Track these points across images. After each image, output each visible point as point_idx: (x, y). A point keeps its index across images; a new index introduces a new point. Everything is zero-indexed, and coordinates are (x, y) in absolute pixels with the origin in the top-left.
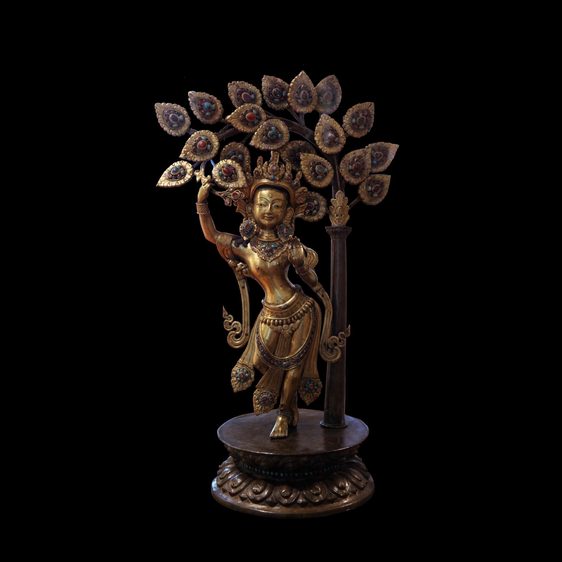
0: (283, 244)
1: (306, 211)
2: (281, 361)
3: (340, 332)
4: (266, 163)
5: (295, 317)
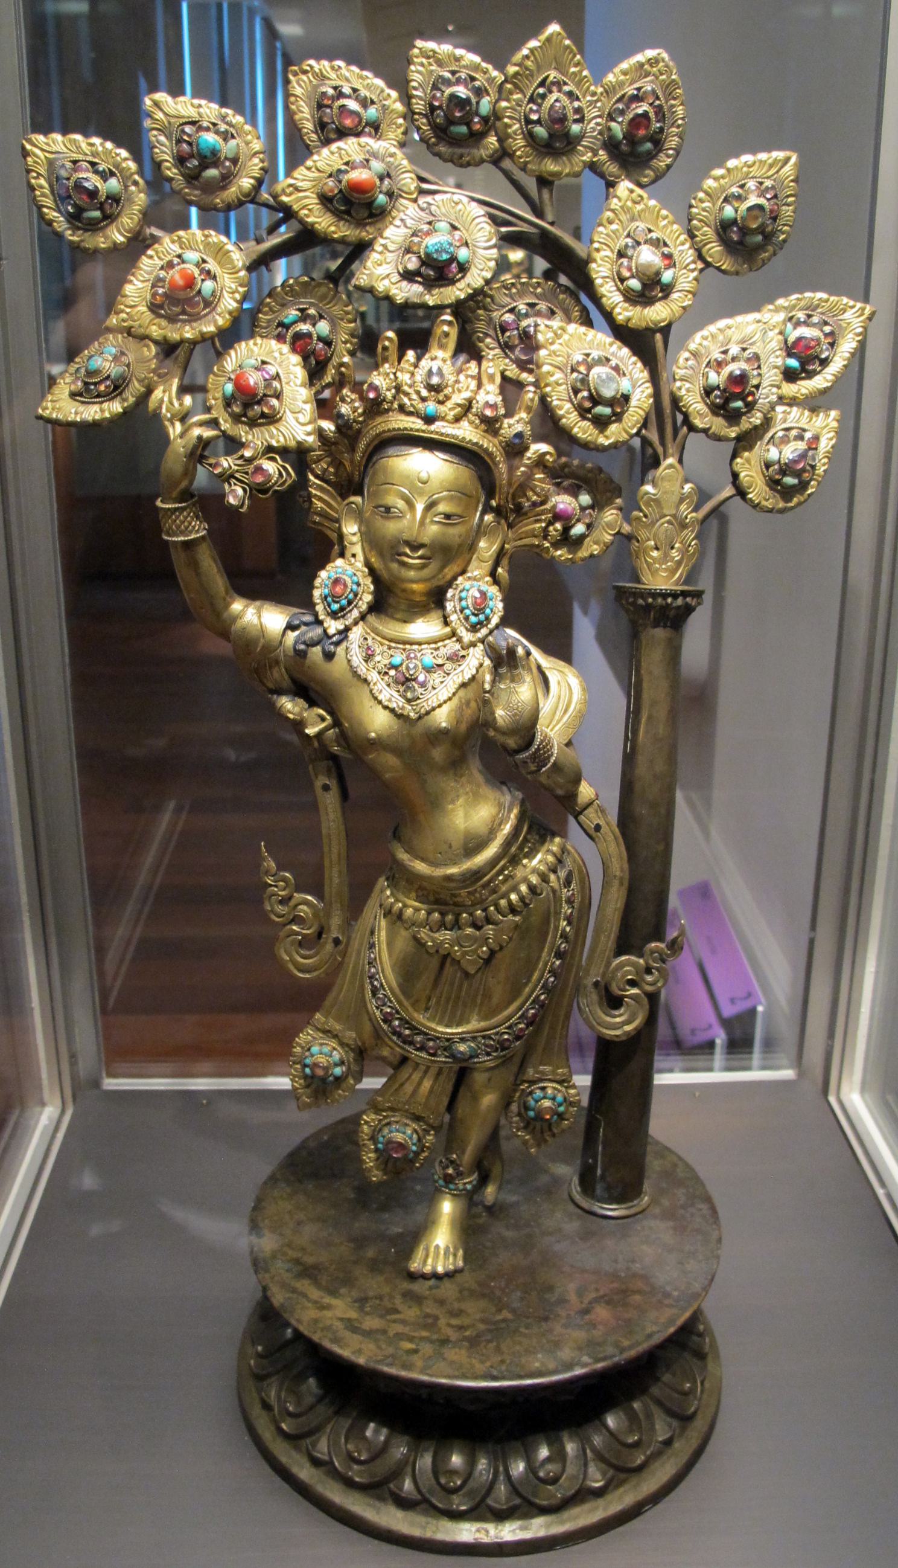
0: (463, 653)
1: (551, 528)
2: (448, 1040)
3: (650, 941)
4: (411, 355)
5: (503, 902)
